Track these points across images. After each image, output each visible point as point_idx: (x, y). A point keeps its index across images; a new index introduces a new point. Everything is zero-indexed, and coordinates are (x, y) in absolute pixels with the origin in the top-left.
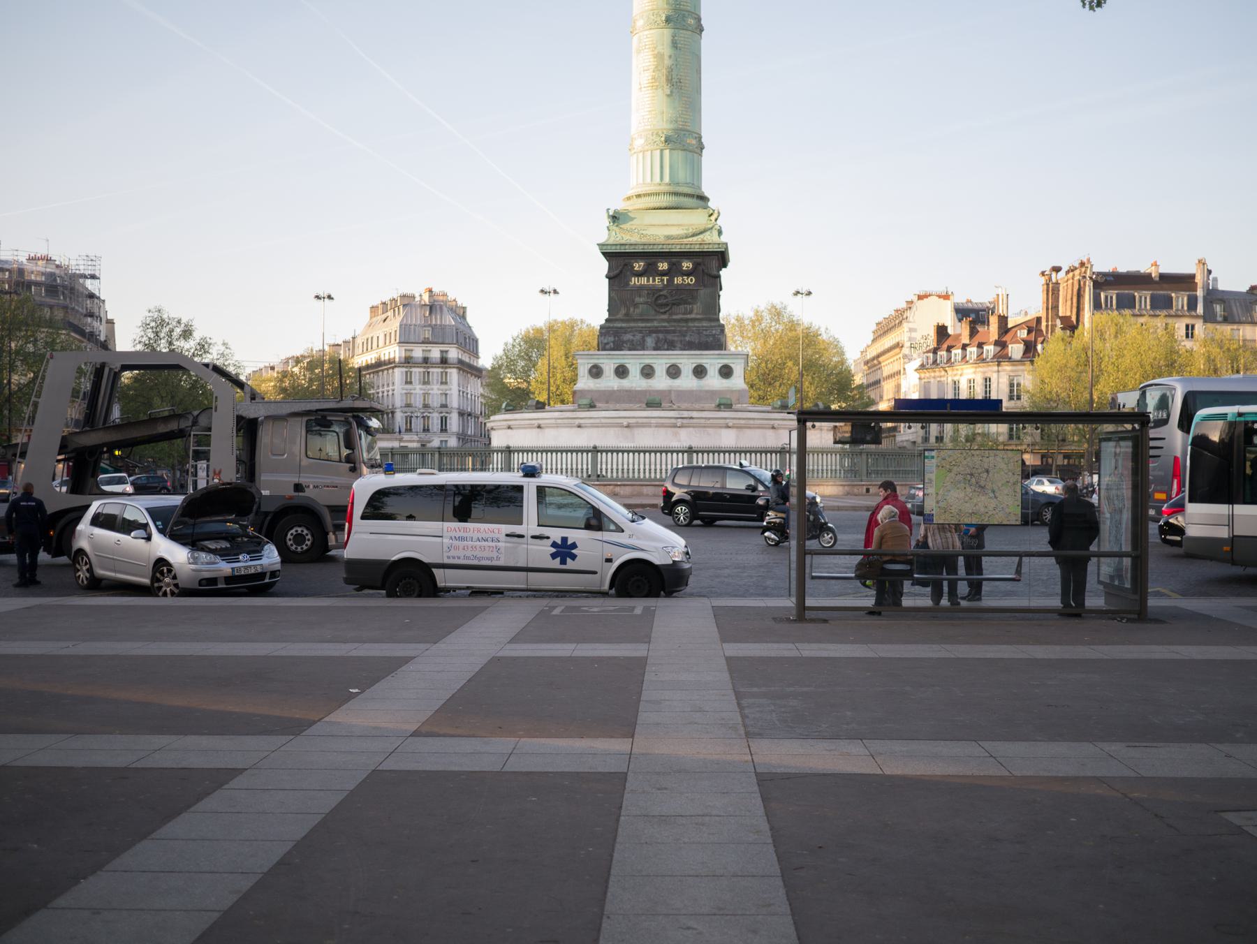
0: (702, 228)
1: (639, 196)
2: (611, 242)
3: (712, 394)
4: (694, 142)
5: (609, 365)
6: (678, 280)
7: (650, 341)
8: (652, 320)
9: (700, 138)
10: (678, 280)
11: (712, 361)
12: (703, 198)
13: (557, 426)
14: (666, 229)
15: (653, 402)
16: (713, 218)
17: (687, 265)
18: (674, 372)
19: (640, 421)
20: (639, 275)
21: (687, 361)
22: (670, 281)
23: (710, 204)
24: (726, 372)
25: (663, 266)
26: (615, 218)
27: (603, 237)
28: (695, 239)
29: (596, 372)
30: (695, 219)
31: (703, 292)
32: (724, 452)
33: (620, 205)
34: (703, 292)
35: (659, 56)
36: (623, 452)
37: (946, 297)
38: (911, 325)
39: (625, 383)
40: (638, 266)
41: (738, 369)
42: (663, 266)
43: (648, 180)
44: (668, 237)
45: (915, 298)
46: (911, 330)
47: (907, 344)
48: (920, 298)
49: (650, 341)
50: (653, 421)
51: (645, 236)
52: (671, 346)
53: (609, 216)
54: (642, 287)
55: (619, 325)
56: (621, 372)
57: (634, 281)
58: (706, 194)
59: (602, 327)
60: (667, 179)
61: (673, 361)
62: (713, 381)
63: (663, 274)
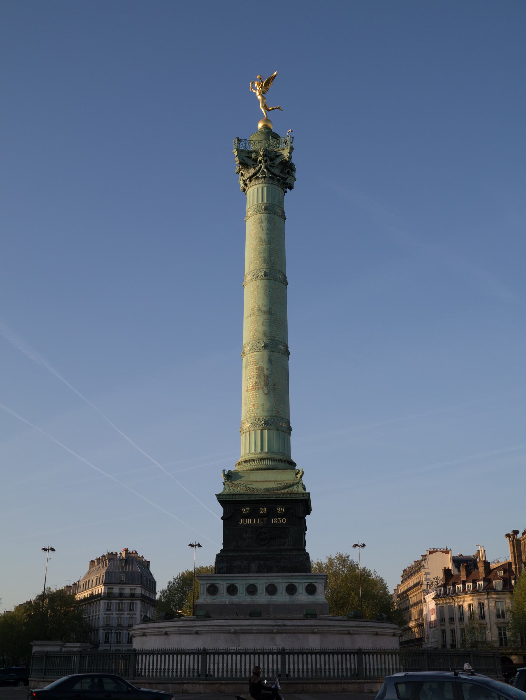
0: (291, 482)
1: (246, 461)
2: (226, 493)
3: (301, 606)
4: (284, 425)
5: (222, 585)
6: (274, 521)
7: (254, 566)
9: (289, 423)
10: (274, 521)
12: (292, 465)
13: (179, 633)
15: (255, 612)
16: (299, 476)
17: (280, 510)
18: (271, 590)
19: (244, 628)
20: (246, 517)
21: (281, 582)
22: (269, 521)
24: (311, 590)
25: (263, 510)
26: (230, 476)
27: (220, 489)
28: (286, 490)
29: (213, 590)
30: (287, 476)
32: (311, 654)
33: (233, 468)
36: (232, 654)
37: (447, 552)
38: (426, 570)
39: (235, 599)
40: (245, 510)
41: (320, 587)
42: (263, 510)
43: (253, 451)
44: (267, 489)
45: (428, 553)
46: (427, 573)
47: (425, 583)
48: (431, 553)
49: (254, 566)
50: (255, 628)
51: (250, 488)
52: (270, 570)
53: (225, 475)
54: (248, 526)
55: (231, 554)
56: (232, 590)
57: (242, 521)
58: (294, 461)
59: (218, 555)
60: (266, 450)
61: (271, 581)
63: (263, 516)
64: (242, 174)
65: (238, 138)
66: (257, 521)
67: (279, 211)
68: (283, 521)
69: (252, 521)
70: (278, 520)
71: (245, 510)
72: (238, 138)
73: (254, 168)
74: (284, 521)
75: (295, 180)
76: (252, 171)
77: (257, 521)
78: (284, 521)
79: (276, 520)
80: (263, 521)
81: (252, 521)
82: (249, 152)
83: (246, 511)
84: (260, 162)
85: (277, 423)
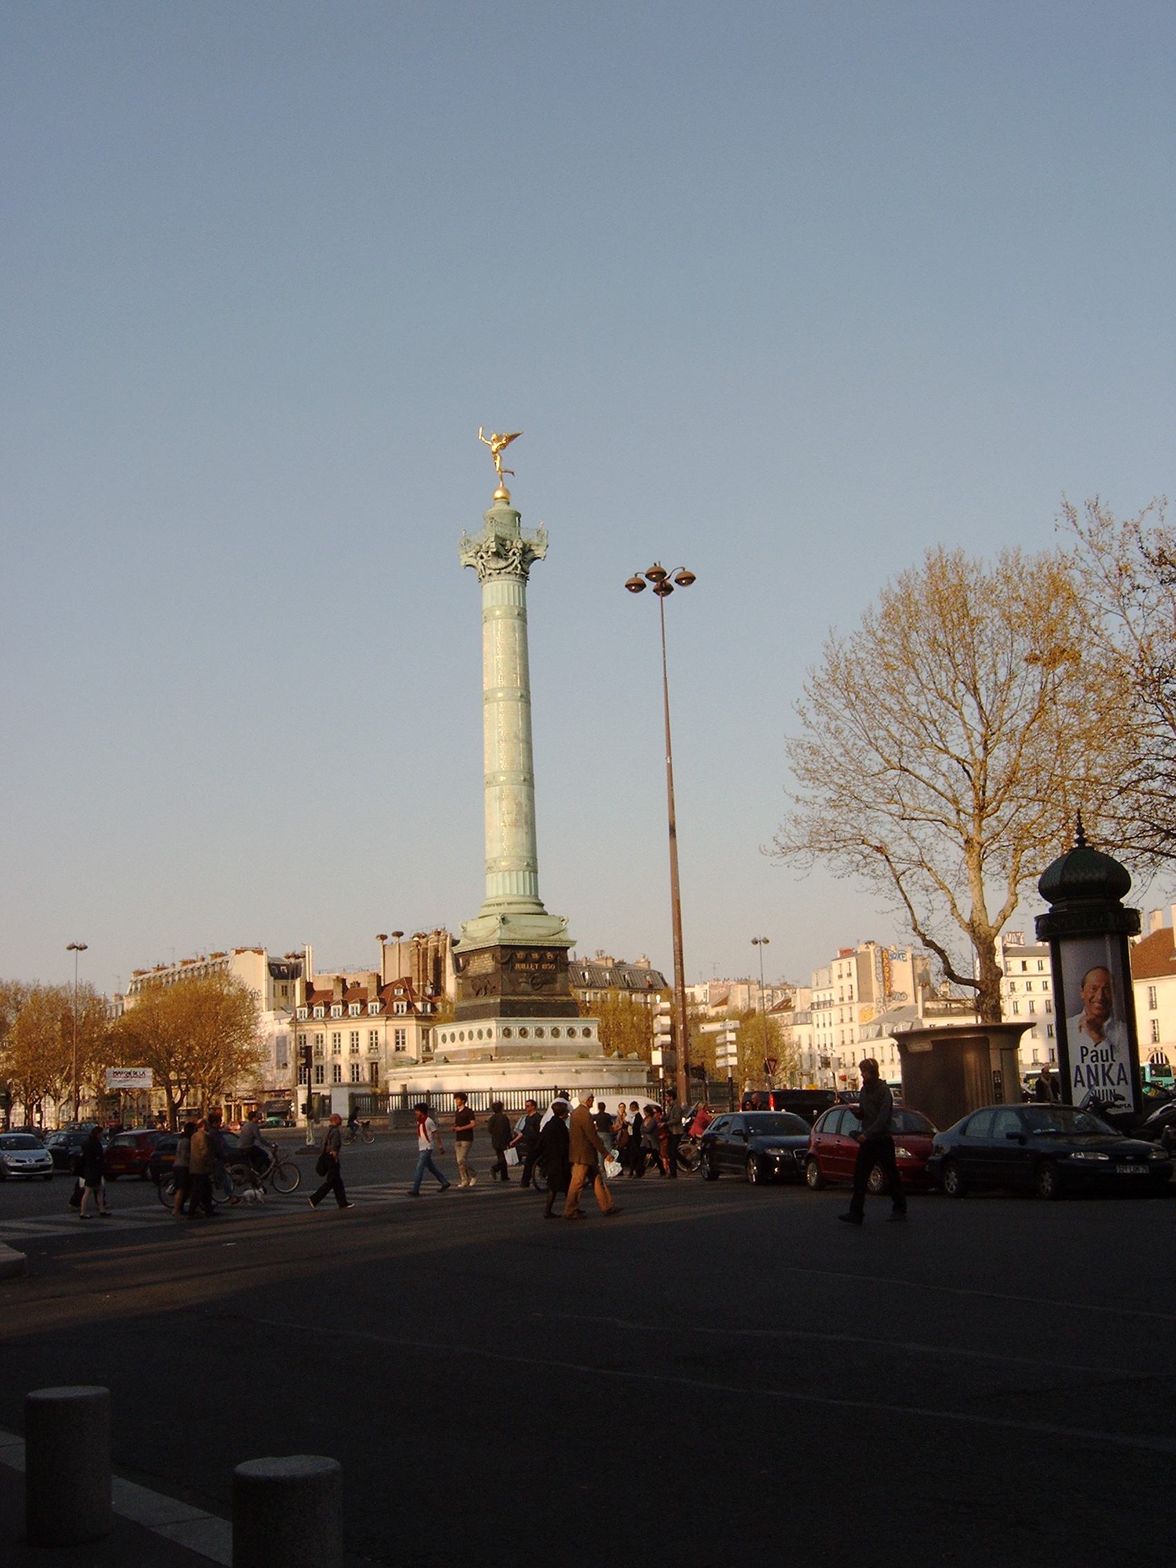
8: (529, 995)
11: (579, 1025)
14: (530, 931)
17: (549, 955)
20: (521, 962)
24: (587, 1033)
25: (536, 956)
31: (560, 976)
34: (560, 976)
35: (519, 805)
37: (260, 953)
40: (520, 955)
42: (536, 956)
44: (540, 936)
54: (522, 971)
57: (518, 966)
64: (482, 557)
71: (520, 955)
73: (507, 559)
76: (502, 564)
82: (504, 540)
84: (514, 554)
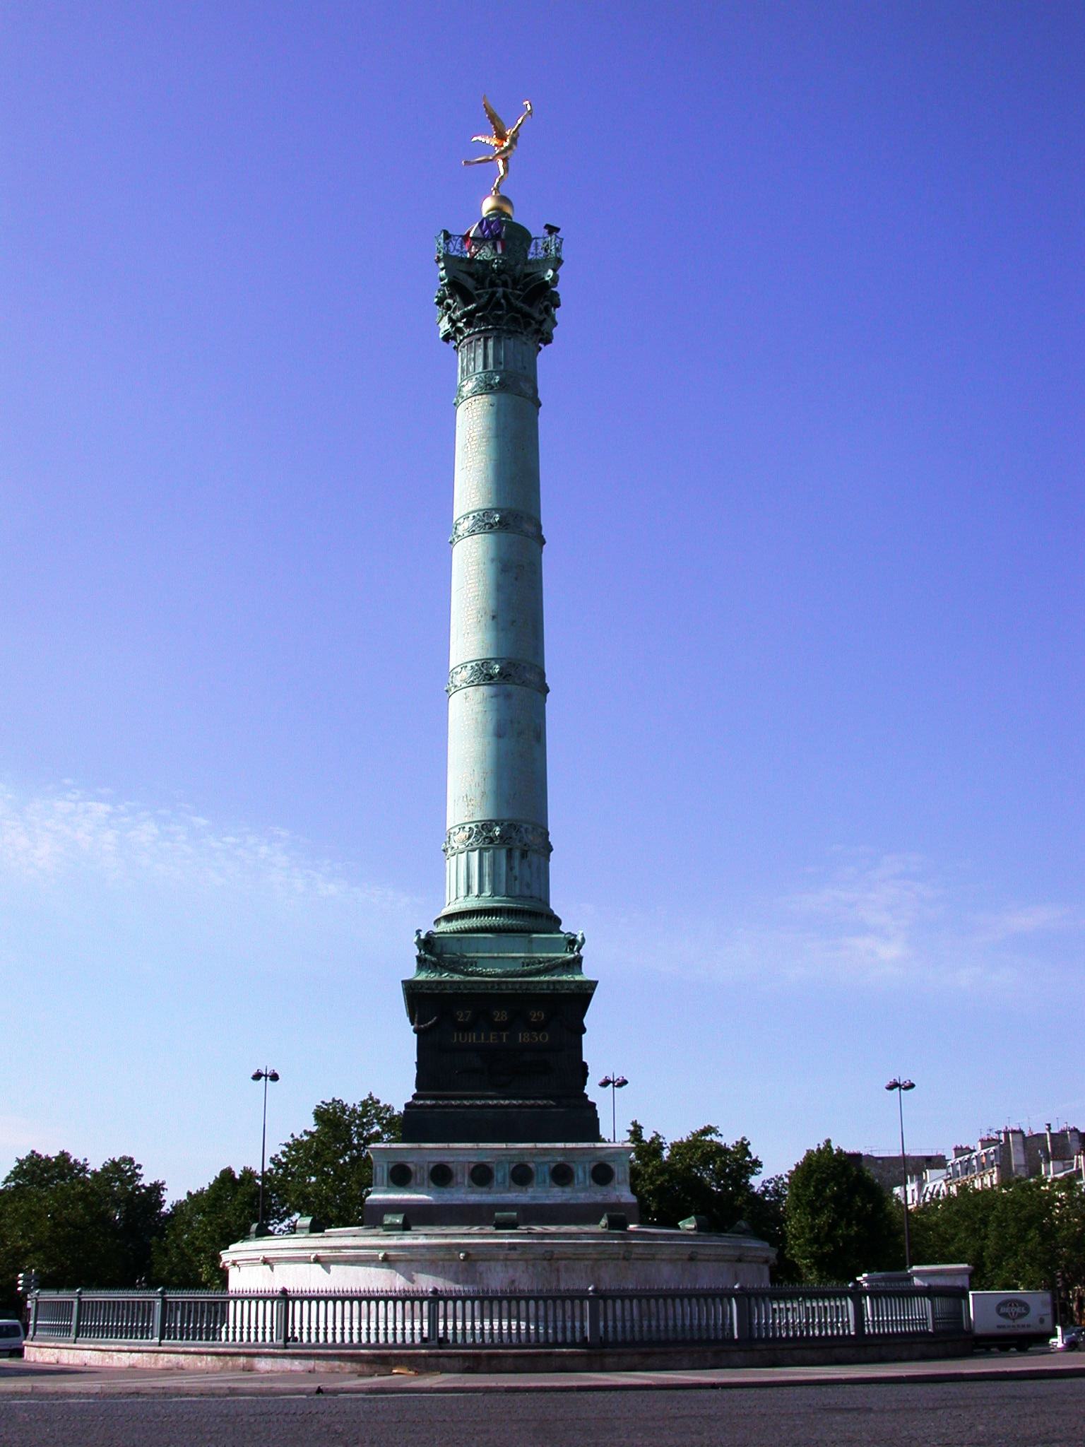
14: (498, 962)
17: (536, 1015)
23: (561, 928)
25: (500, 1016)
40: (462, 1016)
42: (500, 1016)
57: (457, 1038)
62: (582, 1193)
65: (445, 232)
66: (487, 1038)
67: (525, 387)
68: (543, 1038)
69: (478, 1038)
70: (531, 1037)
72: (445, 232)
74: (544, 1037)
75: (555, 324)
77: (487, 1038)
78: (544, 1037)
79: (527, 1035)
80: (500, 1038)
81: (478, 1038)
83: (465, 1016)
85: (517, 837)
